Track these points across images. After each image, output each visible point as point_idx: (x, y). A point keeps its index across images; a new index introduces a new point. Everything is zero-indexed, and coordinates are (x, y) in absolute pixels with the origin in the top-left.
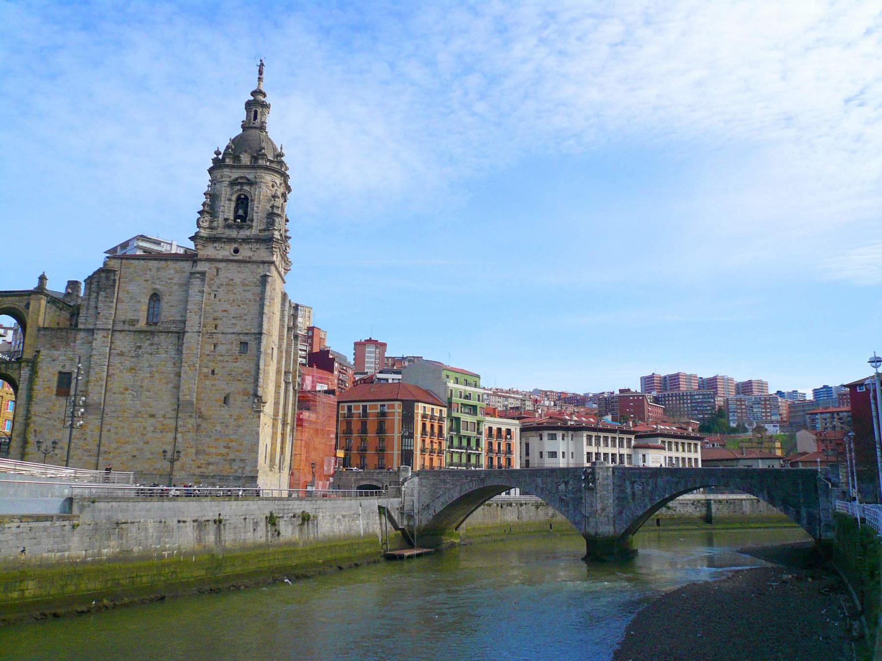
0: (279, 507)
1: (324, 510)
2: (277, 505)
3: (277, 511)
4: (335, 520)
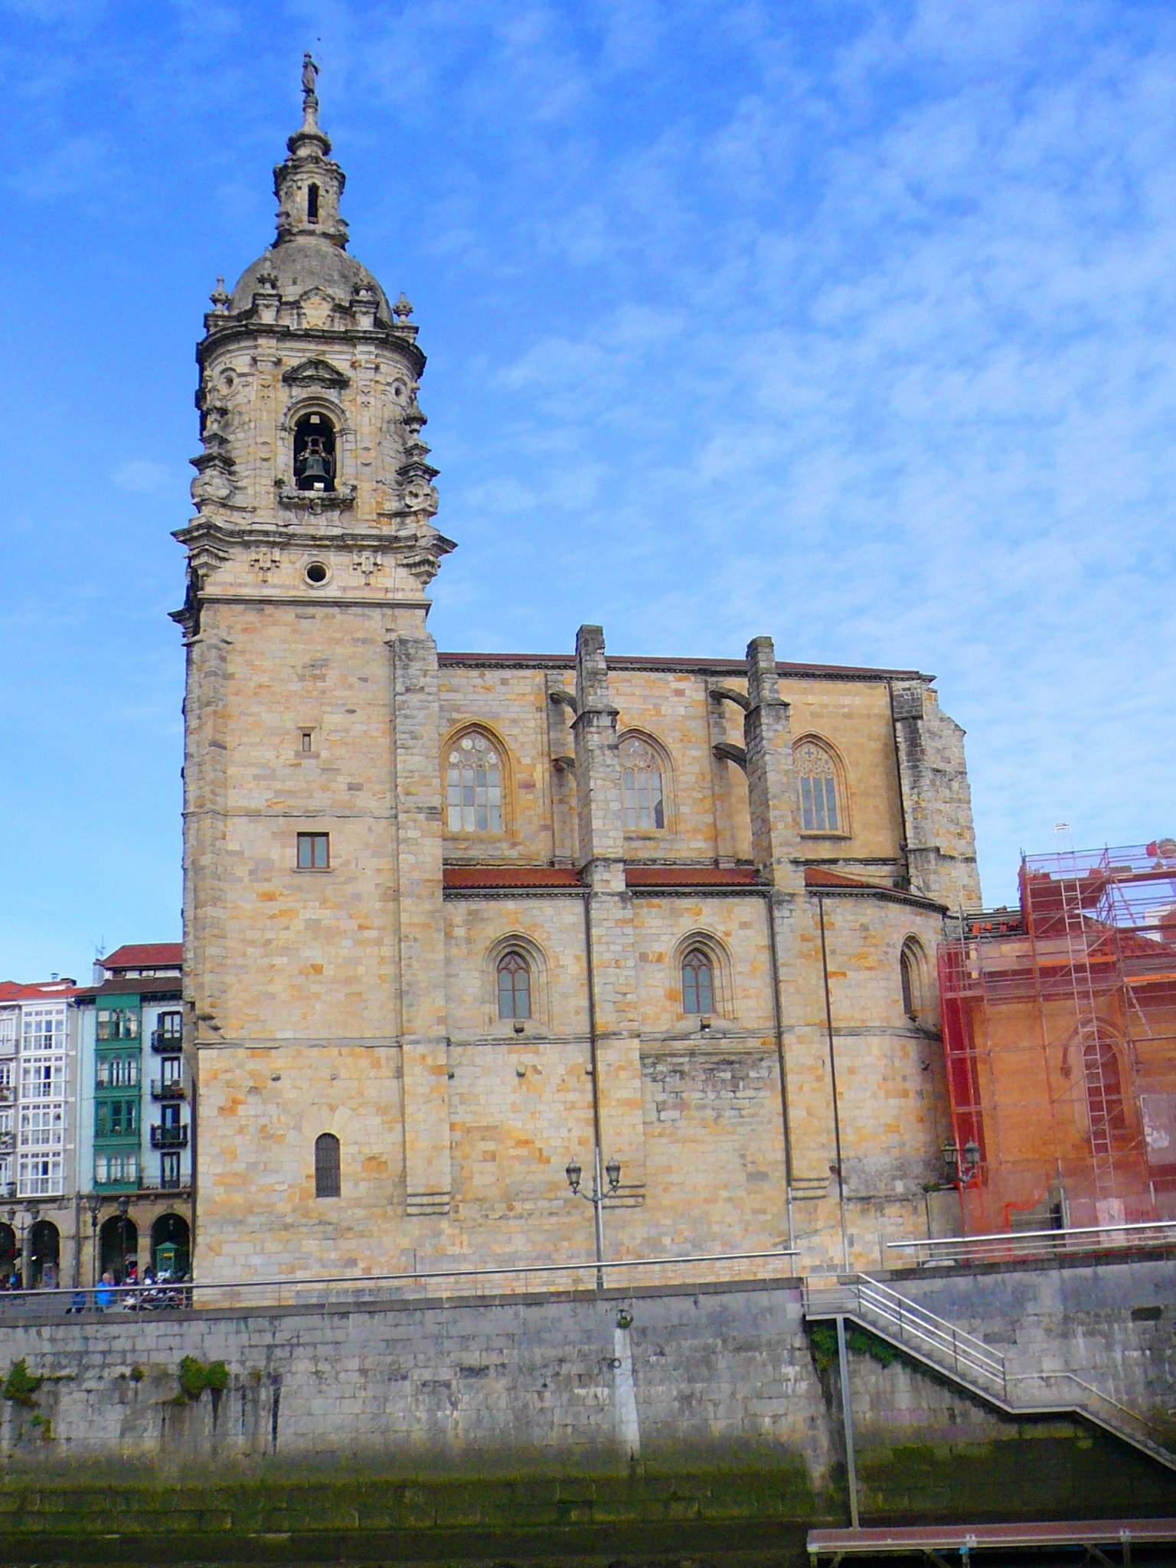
0: (60, 1347)
1: (322, 1350)
2: (52, 1340)
3: (49, 1359)
4: (407, 1387)
